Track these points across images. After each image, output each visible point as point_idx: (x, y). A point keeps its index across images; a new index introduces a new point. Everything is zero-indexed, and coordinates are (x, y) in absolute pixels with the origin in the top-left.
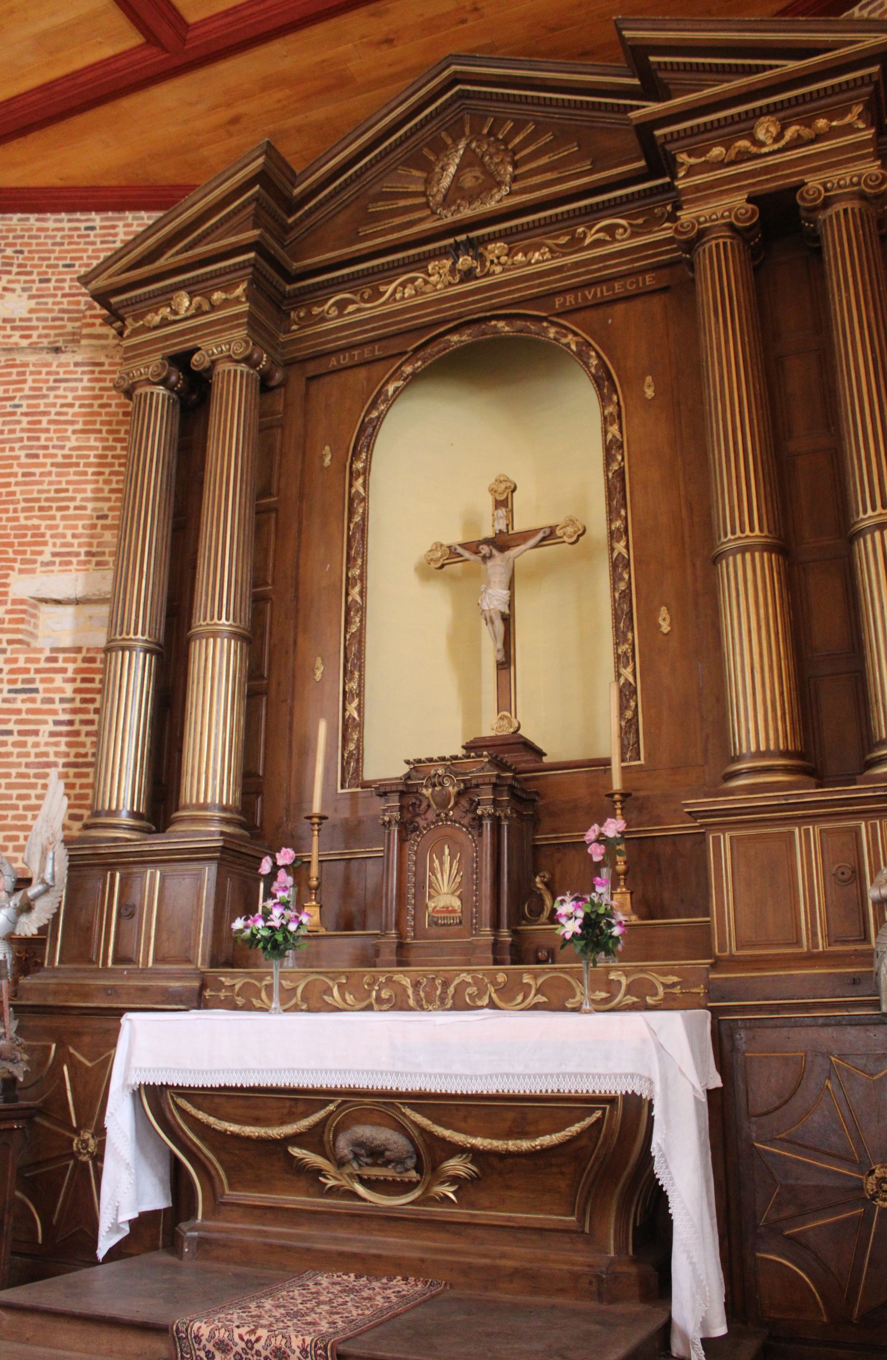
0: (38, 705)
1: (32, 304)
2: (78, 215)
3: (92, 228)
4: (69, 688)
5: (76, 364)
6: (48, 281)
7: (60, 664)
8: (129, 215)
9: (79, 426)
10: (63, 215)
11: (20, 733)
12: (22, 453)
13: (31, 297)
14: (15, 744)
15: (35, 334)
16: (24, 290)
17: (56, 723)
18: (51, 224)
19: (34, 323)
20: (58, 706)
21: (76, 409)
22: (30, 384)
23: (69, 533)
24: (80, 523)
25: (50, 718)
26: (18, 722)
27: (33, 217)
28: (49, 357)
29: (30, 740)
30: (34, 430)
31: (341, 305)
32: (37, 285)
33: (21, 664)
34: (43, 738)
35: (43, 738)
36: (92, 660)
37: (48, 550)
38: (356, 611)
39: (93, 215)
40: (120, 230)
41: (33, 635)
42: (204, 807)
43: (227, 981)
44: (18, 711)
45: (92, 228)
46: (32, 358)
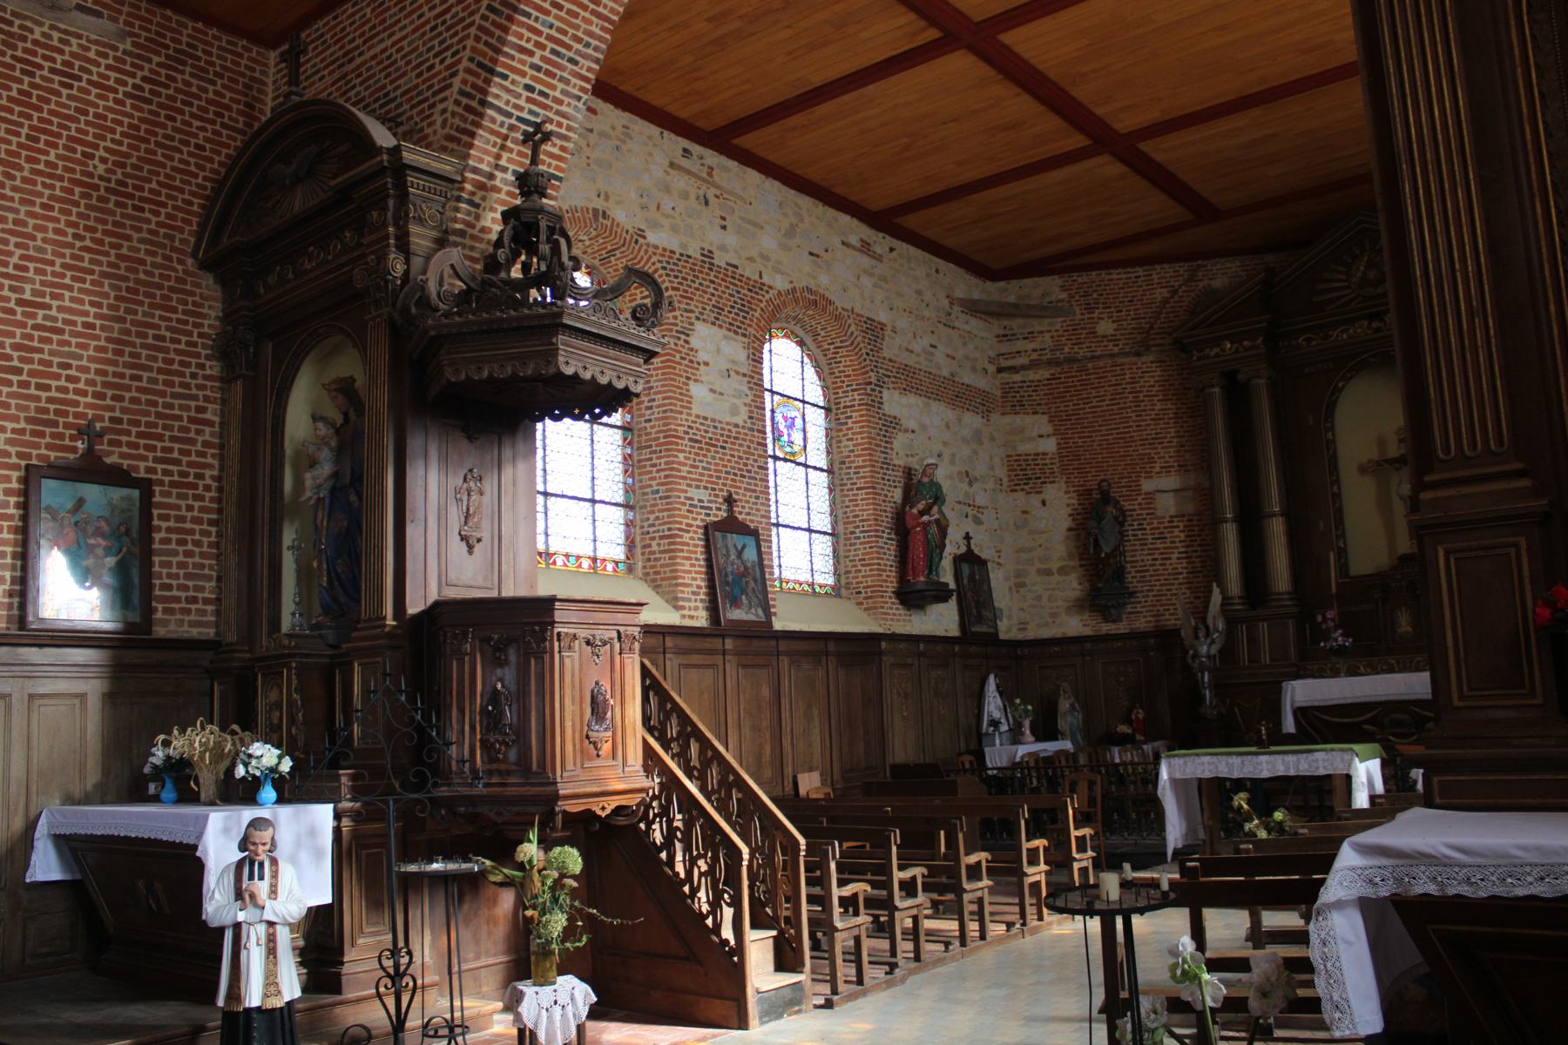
8: (1158, 267)
28: (1135, 359)
31: (1309, 340)
38: (1337, 497)
46: (1126, 360)
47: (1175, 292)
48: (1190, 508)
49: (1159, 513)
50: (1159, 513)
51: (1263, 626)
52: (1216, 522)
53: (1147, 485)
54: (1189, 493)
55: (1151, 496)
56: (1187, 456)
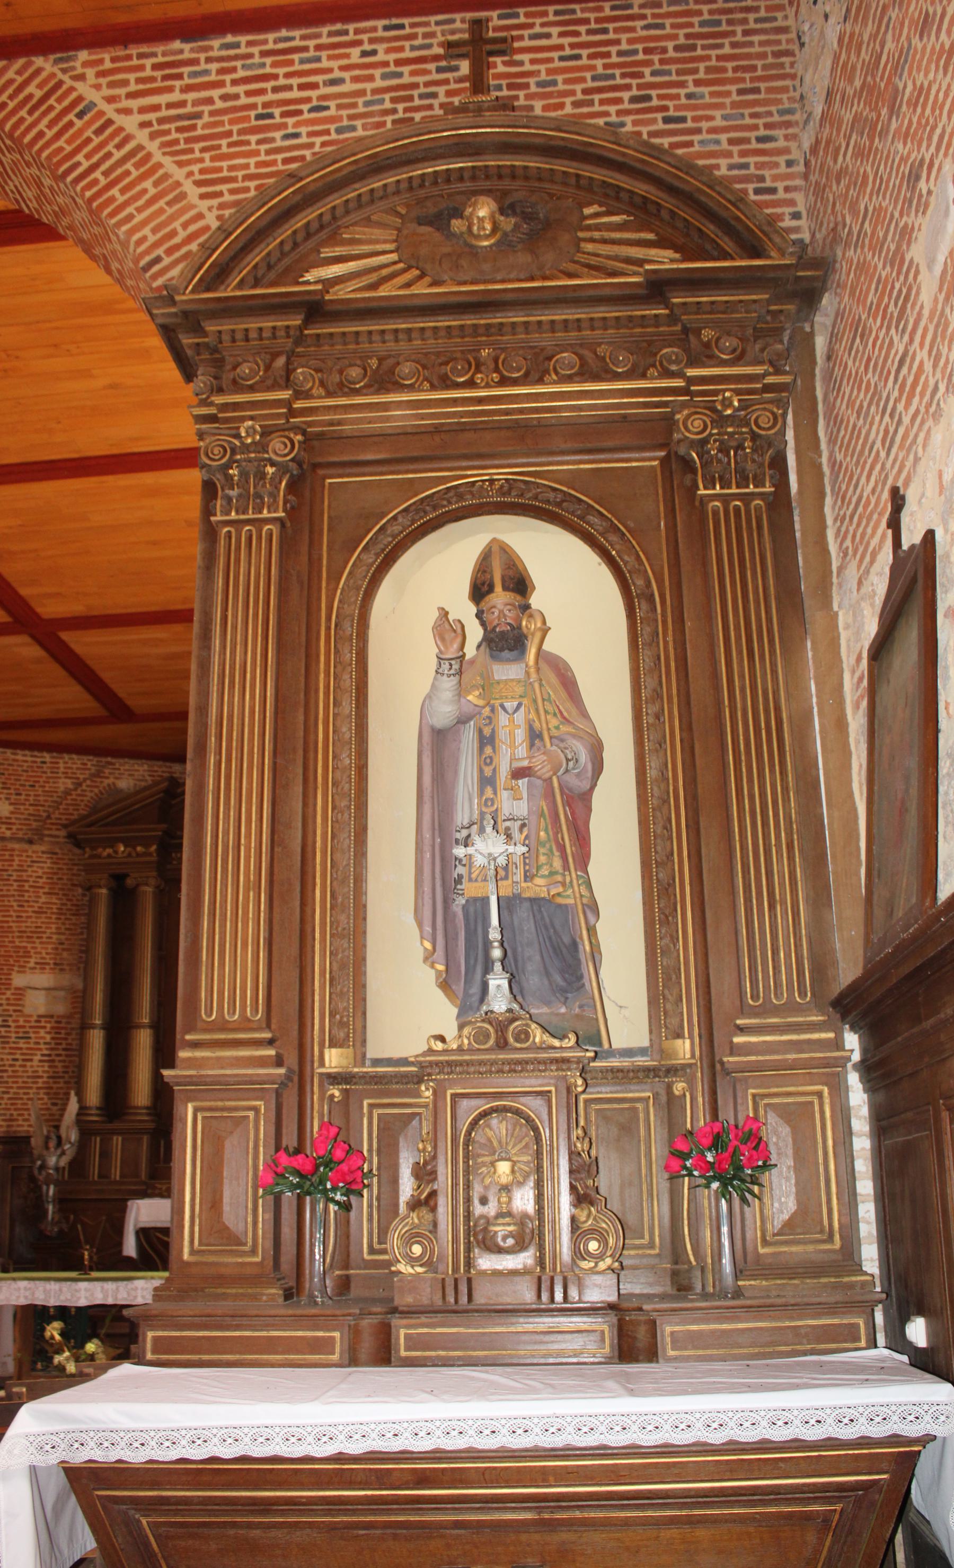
0: (32, 1046)
1: (11, 808)
2: (36, 753)
3: (44, 763)
4: (48, 1037)
5: (43, 852)
6: (20, 794)
7: (43, 1024)
8: (66, 756)
9: (46, 890)
10: (27, 752)
11: (24, 1060)
12: (15, 904)
13: (11, 804)
14: (21, 1066)
15: (14, 827)
16: (7, 799)
17: (43, 1055)
18: (19, 757)
19: (13, 821)
20: (42, 1046)
21: (44, 880)
22: (16, 863)
23: (44, 951)
24: (50, 946)
25: (39, 1053)
26: (22, 1054)
27: (9, 751)
28: (26, 846)
29: (29, 1064)
30: (21, 890)
32: (14, 797)
33: (21, 1023)
34: (35, 1063)
35: (35, 1063)
36: (59, 1022)
37: (33, 960)
39: (45, 754)
40: (61, 765)
41: (23, 1006)
42: (138, 1108)
43: (159, 1186)
44: (21, 1049)
45: (44, 763)
46: (17, 846)
47: (80, 784)
48: (61, 1009)
49: (27, 1011)
50: (27, 1011)
51: (117, 1141)
52: (85, 1026)
53: (18, 980)
54: (62, 993)
55: (20, 993)
56: (65, 954)
